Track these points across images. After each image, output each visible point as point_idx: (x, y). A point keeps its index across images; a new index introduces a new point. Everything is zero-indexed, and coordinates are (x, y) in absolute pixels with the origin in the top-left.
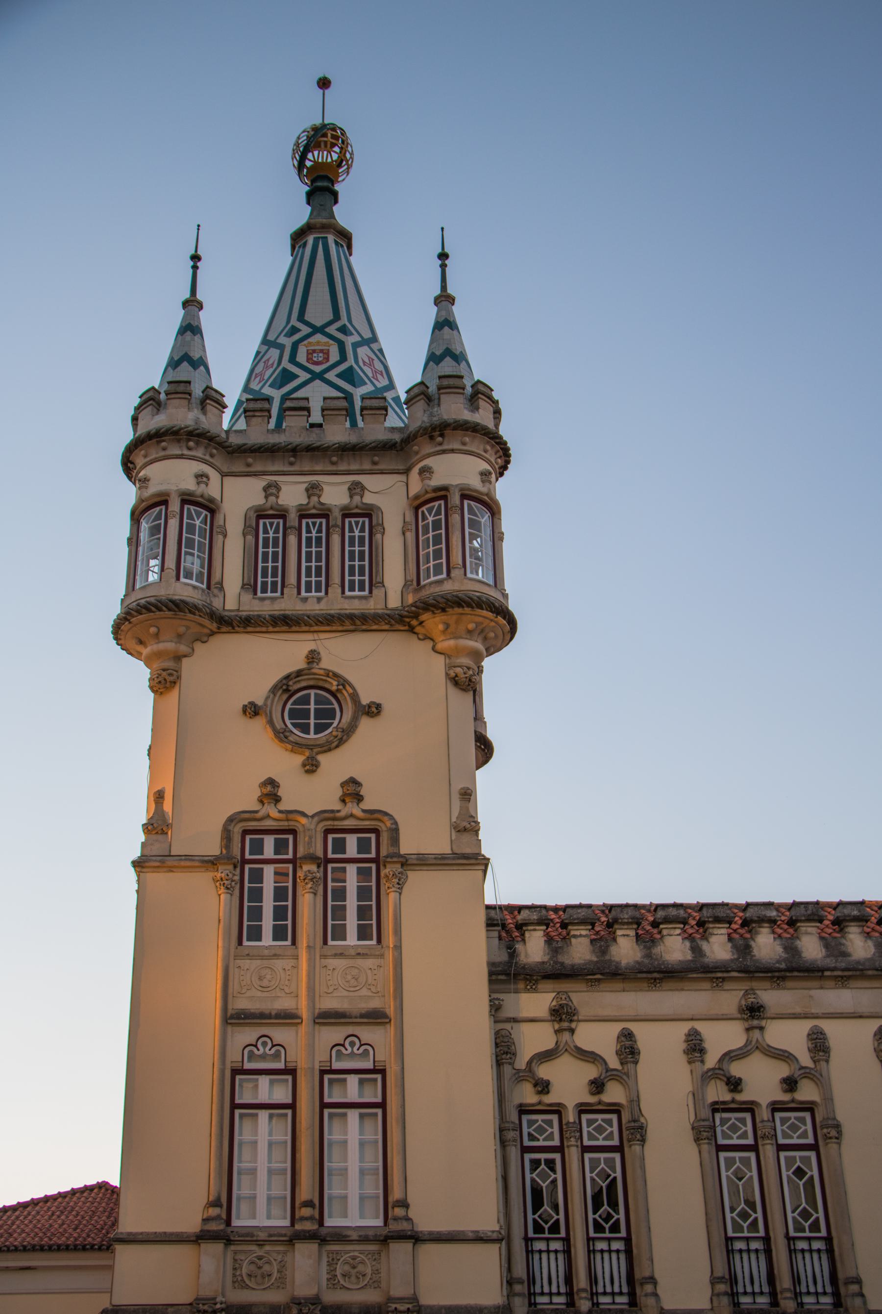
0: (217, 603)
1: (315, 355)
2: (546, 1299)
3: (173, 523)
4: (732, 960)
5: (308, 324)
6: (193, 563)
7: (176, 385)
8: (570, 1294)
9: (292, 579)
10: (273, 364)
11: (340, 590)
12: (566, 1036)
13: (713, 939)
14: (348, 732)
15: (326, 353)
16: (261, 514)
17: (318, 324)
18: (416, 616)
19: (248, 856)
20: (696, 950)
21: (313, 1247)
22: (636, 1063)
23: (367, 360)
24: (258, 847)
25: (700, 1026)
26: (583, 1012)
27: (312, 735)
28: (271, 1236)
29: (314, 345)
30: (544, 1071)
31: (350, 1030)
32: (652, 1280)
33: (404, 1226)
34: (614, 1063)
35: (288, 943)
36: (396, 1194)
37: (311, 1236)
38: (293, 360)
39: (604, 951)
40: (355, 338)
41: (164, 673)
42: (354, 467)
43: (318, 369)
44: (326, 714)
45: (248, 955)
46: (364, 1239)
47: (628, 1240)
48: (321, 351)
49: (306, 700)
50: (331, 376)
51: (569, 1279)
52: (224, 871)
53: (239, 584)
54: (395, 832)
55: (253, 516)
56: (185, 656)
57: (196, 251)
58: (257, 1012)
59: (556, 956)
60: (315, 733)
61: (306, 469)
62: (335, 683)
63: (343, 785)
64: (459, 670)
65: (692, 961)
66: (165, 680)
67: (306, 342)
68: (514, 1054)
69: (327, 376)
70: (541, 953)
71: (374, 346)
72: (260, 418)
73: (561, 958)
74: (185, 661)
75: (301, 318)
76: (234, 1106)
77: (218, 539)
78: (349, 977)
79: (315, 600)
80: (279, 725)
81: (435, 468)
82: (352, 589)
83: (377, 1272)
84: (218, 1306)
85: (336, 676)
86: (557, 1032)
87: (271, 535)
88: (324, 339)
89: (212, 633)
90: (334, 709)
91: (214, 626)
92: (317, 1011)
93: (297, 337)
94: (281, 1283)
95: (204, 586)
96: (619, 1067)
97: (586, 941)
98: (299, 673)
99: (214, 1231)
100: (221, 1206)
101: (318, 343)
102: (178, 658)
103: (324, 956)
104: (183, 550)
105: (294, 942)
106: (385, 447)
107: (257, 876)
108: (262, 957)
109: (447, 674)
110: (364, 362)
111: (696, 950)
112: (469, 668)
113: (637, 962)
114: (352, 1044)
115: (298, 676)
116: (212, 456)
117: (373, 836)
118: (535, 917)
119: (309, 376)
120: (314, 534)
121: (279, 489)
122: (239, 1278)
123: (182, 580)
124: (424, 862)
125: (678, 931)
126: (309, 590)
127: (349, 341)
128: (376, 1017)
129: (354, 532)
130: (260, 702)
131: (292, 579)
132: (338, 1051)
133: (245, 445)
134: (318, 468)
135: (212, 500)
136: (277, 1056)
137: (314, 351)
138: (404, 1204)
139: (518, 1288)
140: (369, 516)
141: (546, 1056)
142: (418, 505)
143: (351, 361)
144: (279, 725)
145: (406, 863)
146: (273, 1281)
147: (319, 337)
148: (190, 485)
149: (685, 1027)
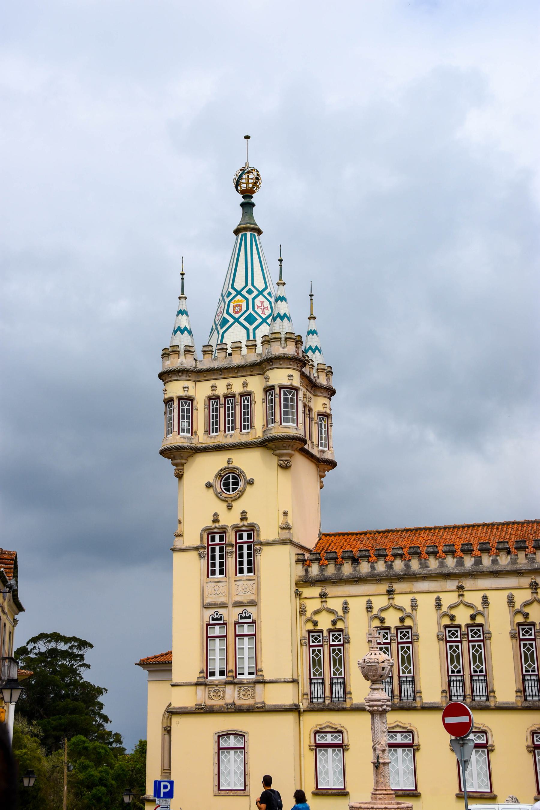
0: (194, 442)
1: (236, 308)
2: (316, 700)
4: (385, 571)
7: (173, 347)
8: (324, 698)
9: (222, 427)
11: (239, 430)
12: (324, 604)
13: (379, 563)
14: (243, 492)
15: (240, 306)
16: (210, 398)
18: (264, 443)
19: (210, 543)
20: (373, 568)
25: (372, 598)
27: (231, 493)
28: (219, 682)
32: (350, 693)
33: (260, 678)
34: (340, 613)
35: (224, 576)
37: (231, 683)
38: (228, 313)
39: (339, 569)
40: (256, 293)
43: (237, 316)
44: (236, 483)
45: (210, 582)
48: (239, 305)
49: (228, 478)
51: (324, 693)
52: (201, 551)
54: (259, 531)
57: (182, 271)
58: (214, 603)
59: (322, 572)
60: (232, 492)
61: (226, 376)
62: (238, 471)
63: (242, 513)
64: (282, 462)
65: (370, 572)
66: (179, 474)
67: (233, 301)
68: (306, 611)
70: (317, 571)
71: (265, 293)
72: (208, 355)
73: (324, 573)
74: (185, 465)
75: (233, 288)
76: (207, 637)
77: (195, 412)
78: (244, 588)
79: (230, 436)
80: (219, 490)
84: (203, 706)
85: (237, 469)
86: (322, 602)
89: (194, 453)
90: (239, 481)
91: (194, 451)
92: (233, 602)
95: (189, 435)
96: (342, 615)
97: (333, 566)
98: (225, 469)
99: (200, 682)
100: (204, 673)
101: (238, 300)
102: (183, 465)
103: (235, 581)
104: (180, 420)
105: (226, 576)
106: (253, 366)
107: (213, 550)
108: (215, 582)
109: (278, 464)
110: (258, 306)
111: (373, 568)
112: (286, 461)
113: (351, 574)
114: (245, 613)
116: (189, 376)
117: (252, 532)
118: (314, 558)
120: (230, 405)
121: (216, 387)
122: (211, 697)
123: (181, 434)
124: (268, 544)
125: (366, 560)
126: (229, 431)
127: (250, 297)
128: (253, 604)
130: (211, 482)
131: (222, 427)
132: (241, 616)
133: (202, 369)
134: (230, 376)
135: (190, 397)
136: (221, 619)
137: (236, 306)
139: (305, 697)
141: (317, 612)
143: (250, 311)
145: (262, 544)
146: (221, 697)
147: (239, 297)
148: (182, 393)
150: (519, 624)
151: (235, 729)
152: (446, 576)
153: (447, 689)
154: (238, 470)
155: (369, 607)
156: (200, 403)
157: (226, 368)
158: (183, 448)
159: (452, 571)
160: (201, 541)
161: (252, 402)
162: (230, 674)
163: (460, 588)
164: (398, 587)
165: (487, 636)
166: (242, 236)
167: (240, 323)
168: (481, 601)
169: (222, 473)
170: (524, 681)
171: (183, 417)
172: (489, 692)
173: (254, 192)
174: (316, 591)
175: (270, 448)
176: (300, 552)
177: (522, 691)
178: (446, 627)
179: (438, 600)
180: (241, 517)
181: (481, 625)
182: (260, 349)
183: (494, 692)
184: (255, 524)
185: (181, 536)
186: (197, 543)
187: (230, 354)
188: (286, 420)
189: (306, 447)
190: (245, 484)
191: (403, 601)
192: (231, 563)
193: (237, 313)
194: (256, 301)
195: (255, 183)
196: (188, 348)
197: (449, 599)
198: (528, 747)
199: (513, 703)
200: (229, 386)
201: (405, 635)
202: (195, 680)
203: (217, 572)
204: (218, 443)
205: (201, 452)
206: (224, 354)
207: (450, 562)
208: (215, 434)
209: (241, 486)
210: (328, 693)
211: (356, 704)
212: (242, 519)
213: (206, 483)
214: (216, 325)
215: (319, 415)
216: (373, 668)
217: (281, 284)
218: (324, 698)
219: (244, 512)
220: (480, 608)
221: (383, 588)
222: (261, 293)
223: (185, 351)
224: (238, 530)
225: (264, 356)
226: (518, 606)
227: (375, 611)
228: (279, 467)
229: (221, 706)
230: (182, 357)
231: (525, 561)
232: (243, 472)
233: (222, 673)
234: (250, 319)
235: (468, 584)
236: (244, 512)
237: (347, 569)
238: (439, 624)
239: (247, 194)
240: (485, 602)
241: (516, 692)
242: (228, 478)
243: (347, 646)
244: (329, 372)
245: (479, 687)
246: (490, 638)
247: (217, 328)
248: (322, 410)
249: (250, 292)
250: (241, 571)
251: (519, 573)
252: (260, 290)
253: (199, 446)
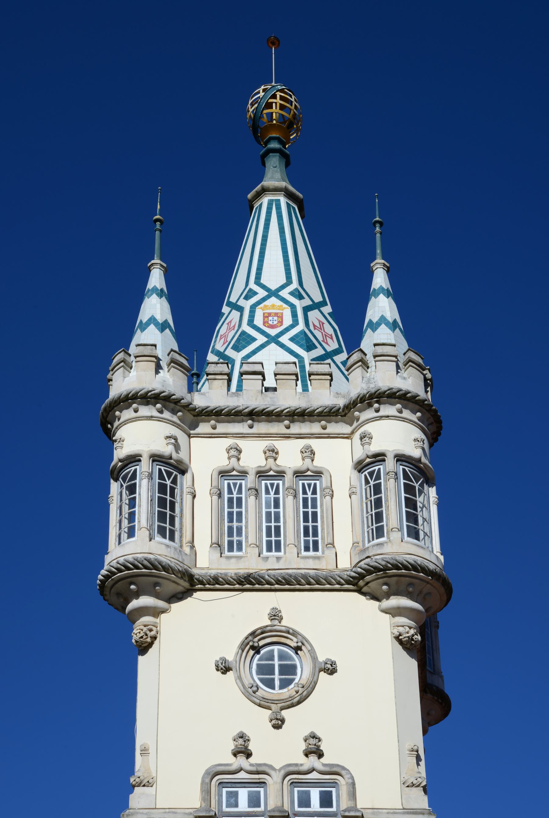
1: (270, 318)
5: (264, 287)
10: (234, 326)
17: (273, 287)
23: (317, 324)
29: (269, 309)
41: (145, 629)
43: (273, 332)
48: (276, 314)
50: (284, 339)
56: (163, 612)
62: (295, 639)
67: (262, 305)
69: (281, 339)
79: (275, 559)
82: (307, 549)
85: (295, 633)
87: (235, 495)
88: (279, 303)
101: (273, 306)
115: (262, 633)
119: (265, 339)
126: (269, 549)
129: (307, 494)
130: (230, 657)
137: (270, 314)
147: (273, 300)
154: (296, 637)
167: (282, 346)
169: (256, 639)
180: (304, 747)
184: (344, 768)
193: (272, 327)
204: (247, 571)
208: (235, 553)
213: (217, 661)
232: (307, 641)
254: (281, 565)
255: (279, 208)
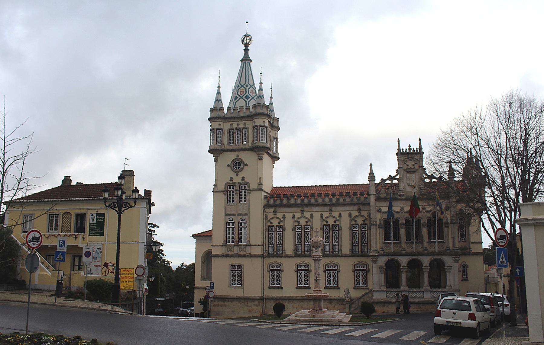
3: (215, 134)
6: (219, 140)
8: (274, 252)
9: (235, 142)
11: (242, 143)
12: (275, 215)
15: (243, 91)
16: (230, 130)
17: (242, 84)
20: (295, 201)
21: (237, 247)
22: (285, 219)
24: (230, 188)
26: (278, 212)
30: (271, 221)
31: (243, 216)
33: (249, 244)
36: (248, 240)
38: (237, 94)
39: (282, 202)
40: (249, 86)
42: (245, 120)
43: (241, 96)
46: (244, 246)
47: (282, 245)
49: (237, 163)
51: (274, 250)
52: (224, 193)
53: (226, 144)
55: (228, 130)
71: (253, 87)
77: (223, 135)
80: (233, 168)
81: (256, 121)
83: (245, 250)
85: (241, 159)
93: (239, 88)
94: (233, 251)
95: (221, 144)
97: (279, 200)
98: (235, 159)
102: (218, 157)
111: (295, 201)
119: (240, 97)
123: (217, 144)
127: (247, 88)
128: (246, 214)
135: (222, 128)
138: (249, 241)
140: (247, 129)
141: (272, 218)
142: (254, 127)
143: (247, 94)
144: (233, 168)
145: (250, 191)
148: (218, 127)
149: (292, 214)
150: (353, 224)
151: (238, 263)
152: (324, 205)
153: (323, 249)
155: (294, 217)
156: (226, 132)
157: (237, 117)
158: (218, 150)
159: (327, 204)
160: (225, 188)
161: (248, 131)
162: (236, 242)
163: (331, 210)
164: (306, 209)
165: (340, 229)
166: (244, 63)
167: (243, 99)
168: (338, 215)
170: (353, 245)
171: (218, 137)
172: (340, 250)
173: (249, 44)
174: (271, 210)
175: (255, 151)
176: (266, 194)
177: (352, 250)
178: (324, 225)
179: (322, 215)
181: (338, 225)
182: (251, 110)
183: (341, 250)
185: (216, 186)
186: (223, 189)
187: (239, 112)
188: (262, 140)
189: (269, 151)
190: (244, 166)
191: (308, 215)
192: (237, 198)
193: (242, 94)
194: (249, 90)
195: (250, 41)
196: (221, 108)
197: (326, 214)
198: (352, 270)
199: (349, 254)
200: (238, 125)
201: (307, 228)
202: (222, 244)
203: (231, 201)
205: (226, 152)
206: (236, 111)
207: (327, 200)
208: (231, 144)
209: (242, 167)
210: (275, 250)
211: (287, 255)
212: (242, 180)
214: (232, 99)
215: (273, 138)
216: (316, 243)
217: (261, 83)
218: (274, 252)
219: (243, 177)
220: (338, 218)
221: (299, 209)
222: (251, 86)
223: (220, 109)
224: (240, 184)
225: (253, 113)
226: (352, 218)
227: (296, 219)
228: (258, 160)
229: (232, 255)
230: (219, 112)
231: (357, 200)
233: (233, 242)
234: (247, 97)
235: (334, 208)
236: (243, 177)
237: (285, 201)
238: (321, 224)
239: (246, 45)
240: (340, 215)
241: (350, 250)
242: (237, 163)
243: (284, 232)
244: (278, 120)
245: (336, 248)
246: (341, 230)
247: (233, 100)
248: (274, 136)
249: (247, 86)
250: (241, 201)
251: (354, 205)
252: (251, 85)
253: (225, 149)
254: (239, 147)
255: (246, 64)
